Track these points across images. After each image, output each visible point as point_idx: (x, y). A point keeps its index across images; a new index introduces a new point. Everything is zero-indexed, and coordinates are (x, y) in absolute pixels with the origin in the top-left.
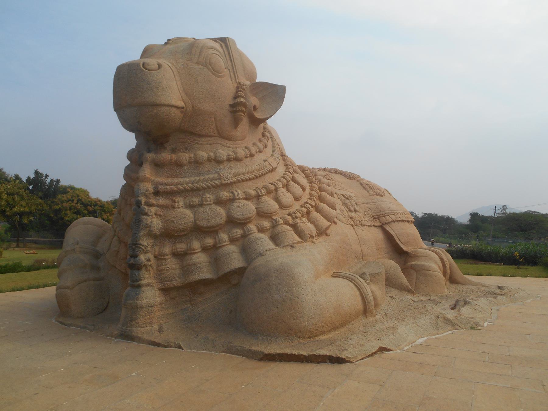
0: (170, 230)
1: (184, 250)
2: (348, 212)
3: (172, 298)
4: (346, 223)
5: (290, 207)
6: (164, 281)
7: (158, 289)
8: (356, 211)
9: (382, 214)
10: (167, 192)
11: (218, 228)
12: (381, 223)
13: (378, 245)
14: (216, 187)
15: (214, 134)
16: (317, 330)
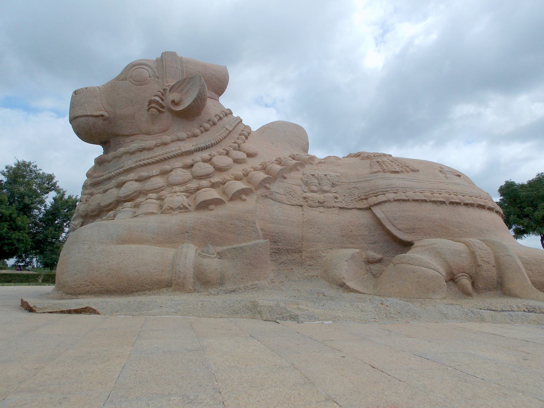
4: (289, 203)
9: (373, 194)
12: (368, 204)
13: (351, 231)
16: (80, 287)
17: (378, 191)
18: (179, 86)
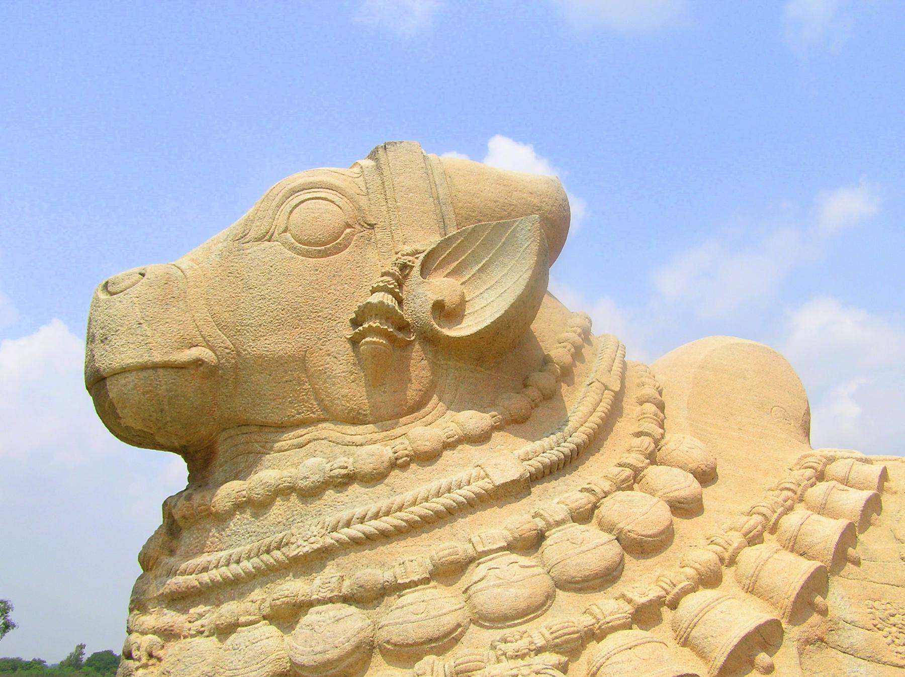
15: (313, 413)
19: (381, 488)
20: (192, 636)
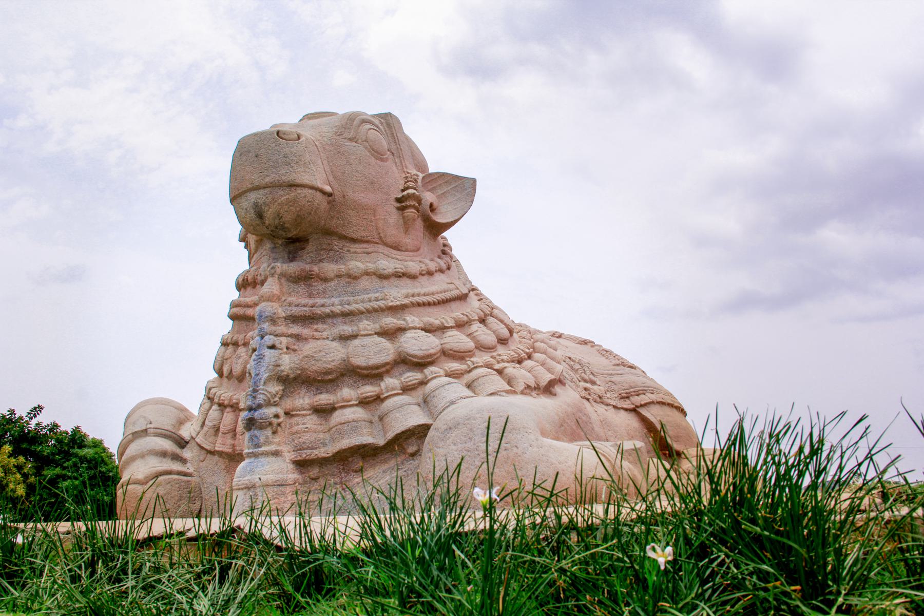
0: (310, 371)
1: (331, 401)
2: (580, 381)
3: (312, 479)
5: (493, 349)
6: (300, 449)
7: (291, 460)
8: (593, 383)
9: (634, 392)
10: (305, 316)
11: (384, 369)
12: (633, 404)
14: (378, 311)
17: (638, 388)
18: (429, 182)
19: (416, 283)
20: (324, 339)
